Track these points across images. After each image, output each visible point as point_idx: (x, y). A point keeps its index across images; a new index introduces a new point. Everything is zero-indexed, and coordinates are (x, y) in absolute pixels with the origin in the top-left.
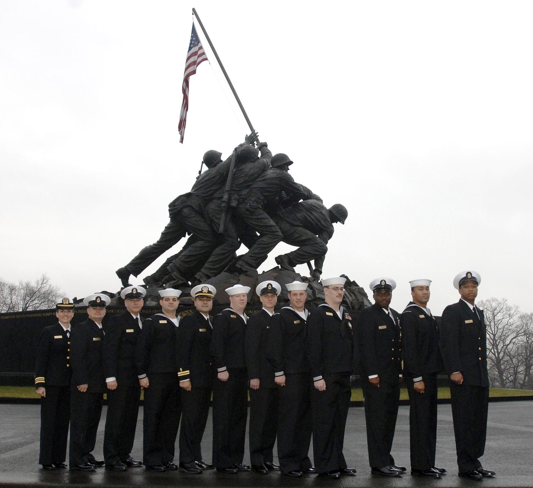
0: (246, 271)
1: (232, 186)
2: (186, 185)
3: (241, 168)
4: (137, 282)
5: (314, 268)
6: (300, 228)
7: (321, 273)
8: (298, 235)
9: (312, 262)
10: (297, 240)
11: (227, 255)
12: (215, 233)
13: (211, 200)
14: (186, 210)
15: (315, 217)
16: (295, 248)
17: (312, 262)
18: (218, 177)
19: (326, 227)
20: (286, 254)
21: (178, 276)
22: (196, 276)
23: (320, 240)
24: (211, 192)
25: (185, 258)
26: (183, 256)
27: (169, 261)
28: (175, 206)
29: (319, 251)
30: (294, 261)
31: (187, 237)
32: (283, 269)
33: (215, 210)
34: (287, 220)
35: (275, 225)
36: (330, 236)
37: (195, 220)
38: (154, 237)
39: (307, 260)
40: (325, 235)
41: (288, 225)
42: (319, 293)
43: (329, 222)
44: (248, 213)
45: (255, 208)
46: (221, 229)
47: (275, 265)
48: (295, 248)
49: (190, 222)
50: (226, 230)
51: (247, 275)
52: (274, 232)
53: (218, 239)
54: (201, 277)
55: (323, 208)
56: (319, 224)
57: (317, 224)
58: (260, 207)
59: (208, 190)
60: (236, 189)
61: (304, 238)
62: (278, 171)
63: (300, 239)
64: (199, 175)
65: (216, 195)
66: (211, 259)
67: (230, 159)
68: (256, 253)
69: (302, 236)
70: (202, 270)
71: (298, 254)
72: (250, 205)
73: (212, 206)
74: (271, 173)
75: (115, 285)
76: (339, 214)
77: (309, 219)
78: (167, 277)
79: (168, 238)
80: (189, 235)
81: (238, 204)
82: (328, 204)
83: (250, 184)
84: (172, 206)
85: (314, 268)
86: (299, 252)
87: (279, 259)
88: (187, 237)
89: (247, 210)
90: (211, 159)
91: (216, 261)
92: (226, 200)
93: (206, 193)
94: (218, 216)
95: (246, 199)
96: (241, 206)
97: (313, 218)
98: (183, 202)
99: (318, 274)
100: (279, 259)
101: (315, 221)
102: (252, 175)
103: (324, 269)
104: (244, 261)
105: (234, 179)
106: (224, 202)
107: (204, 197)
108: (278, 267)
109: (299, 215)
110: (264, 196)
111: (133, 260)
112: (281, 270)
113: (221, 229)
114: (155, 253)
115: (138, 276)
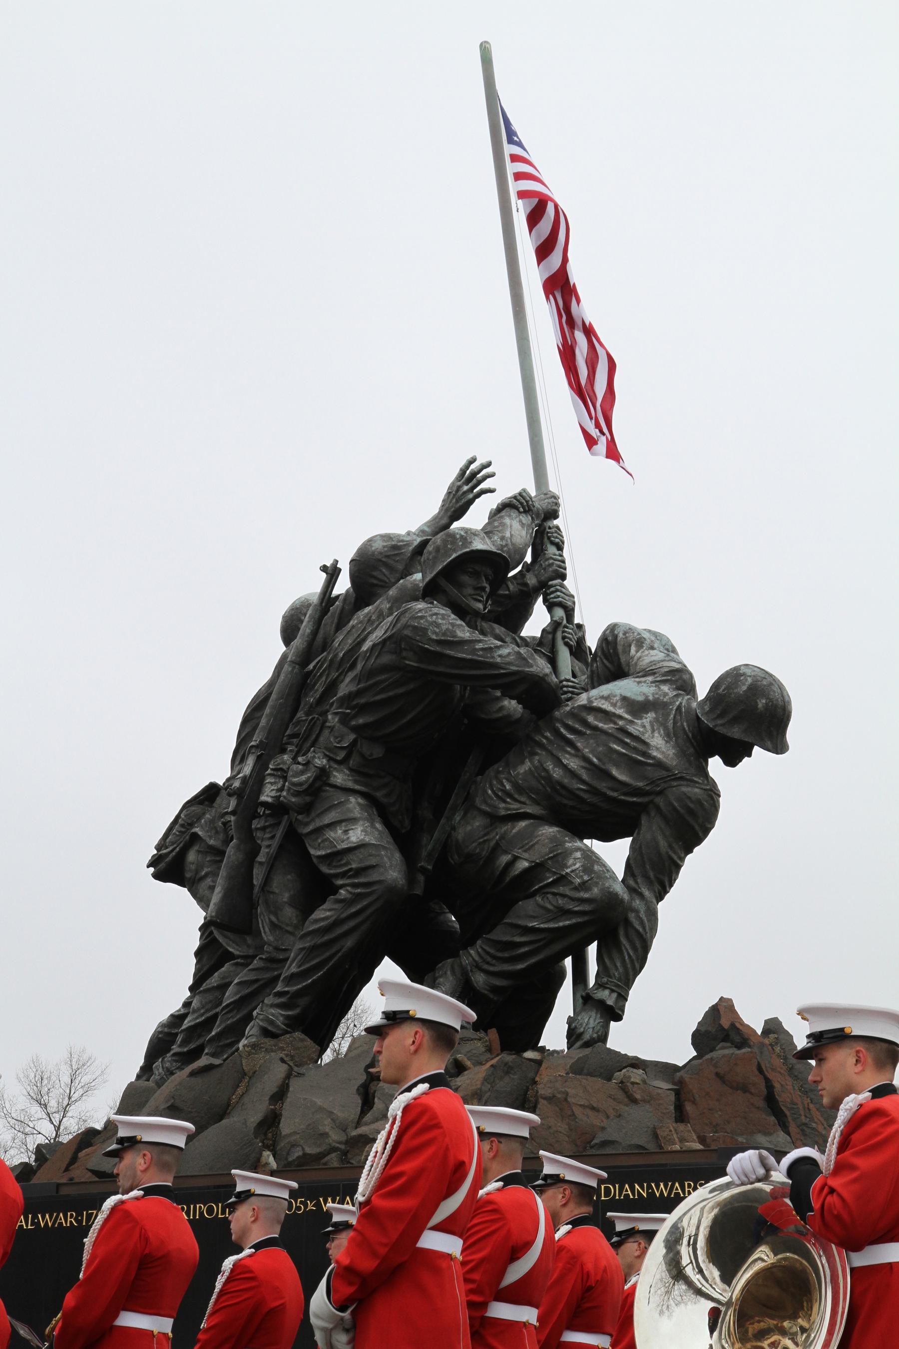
8: (505, 859)
29: (565, 913)
52: (359, 872)
56: (603, 786)
57: (594, 791)
69: (516, 859)
77: (557, 773)
97: (573, 763)
101: (585, 776)
110: (355, 729)
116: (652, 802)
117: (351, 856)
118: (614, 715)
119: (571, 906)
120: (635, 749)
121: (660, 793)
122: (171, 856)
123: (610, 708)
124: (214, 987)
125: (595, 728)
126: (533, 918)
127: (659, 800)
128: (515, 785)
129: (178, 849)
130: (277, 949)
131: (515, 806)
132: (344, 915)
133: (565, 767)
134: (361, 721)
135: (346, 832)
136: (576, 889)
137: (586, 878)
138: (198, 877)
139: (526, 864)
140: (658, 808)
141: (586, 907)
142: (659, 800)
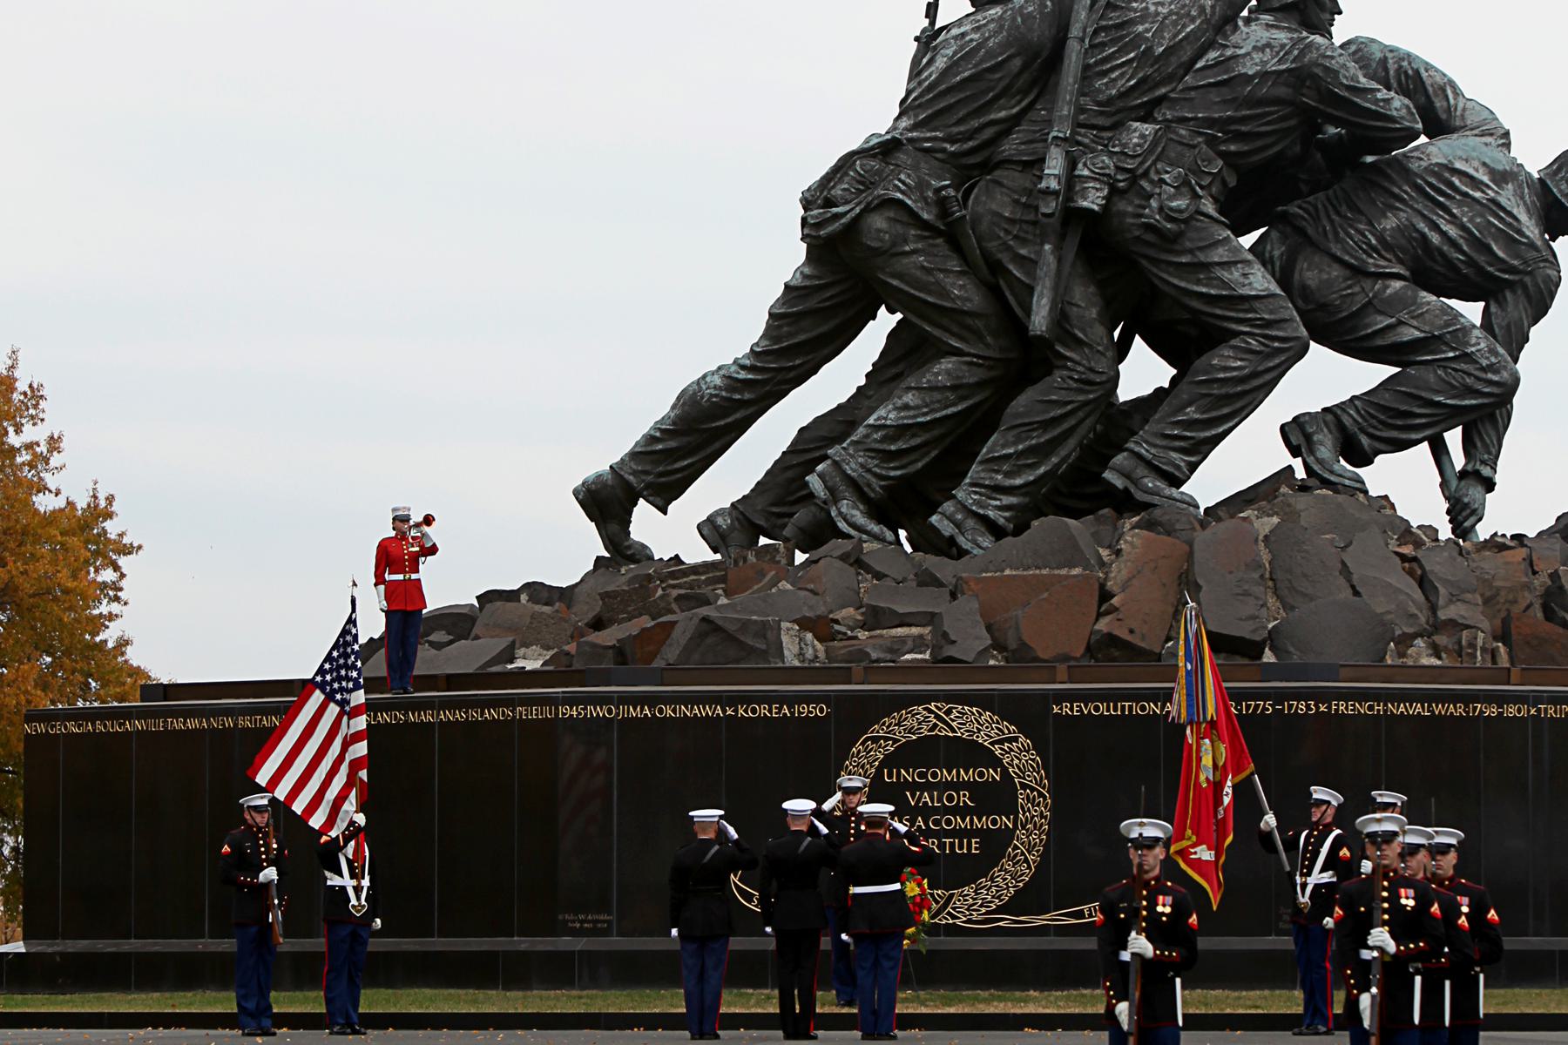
0: (1147, 506)
1: (1081, 110)
3: (1114, 18)
4: (671, 532)
5: (1458, 460)
6: (1398, 284)
7: (1490, 486)
9: (1454, 438)
10: (1379, 342)
11: (1066, 426)
12: (1014, 324)
13: (987, 167)
14: (878, 222)
15: (1463, 228)
16: (1369, 375)
17: (1454, 438)
18: (1017, 63)
19: (1512, 270)
20: (1325, 410)
21: (860, 519)
22: (934, 519)
23: (1479, 343)
24: (988, 133)
25: (883, 440)
26: (876, 428)
28: (829, 203)
30: (1365, 440)
31: (885, 322)
32: (1313, 482)
33: (1011, 221)
34: (1336, 250)
35: (1275, 288)
36: (1540, 305)
37: (919, 258)
38: (734, 333)
39: (1428, 432)
40: (1515, 306)
41: (1336, 272)
42: (1453, 599)
43: (1531, 245)
44: (1149, 237)
45: (1185, 221)
46: (1039, 320)
47: (1279, 457)
48: (1369, 375)
49: (894, 276)
50: (1061, 318)
51: (1150, 525)
52: (1269, 324)
54: (958, 525)
55: (1508, 175)
56: (1481, 259)
57: (1471, 262)
58: (1209, 207)
59: (975, 123)
60: (1101, 121)
61: (1410, 334)
62: (1282, 36)
63: (1391, 338)
64: (926, 22)
65: (1011, 147)
66: (995, 445)
68: (1191, 424)
69: (1400, 323)
70: (960, 494)
71: (1384, 409)
72: (1161, 209)
73: (993, 202)
75: (570, 552)
77: (1435, 238)
78: (802, 515)
80: (892, 311)
81: (1108, 198)
83: (1163, 90)
84: (817, 199)
85: (1458, 460)
86: (1386, 399)
87: (1297, 434)
88: (885, 322)
89: (1149, 227)
91: (1019, 455)
92: (1054, 185)
93: (970, 139)
94: (1023, 252)
95: (1146, 174)
96: (1122, 205)
97: (1452, 231)
98: (866, 184)
99: (1473, 492)
100: (1297, 434)
102: (1169, 51)
103: (1506, 470)
104: (1139, 456)
105: (1088, 74)
106: (1047, 192)
107: (953, 154)
108: (1290, 467)
109: (1389, 223)
110: (1223, 155)
111: (650, 439)
112: (1303, 488)
113: (1039, 320)
114: (743, 404)
115: (673, 507)
116: (1521, 281)
117: (1257, 305)
118: (1482, 182)
119: (1479, 386)
120: (1509, 225)
121: (1530, 273)
122: (852, 214)
123: (1471, 171)
124: (945, 387)
125: (1466, 195)
126: (1438, 392)
127: (1527, 279)
128: (1381, 238)
129: (858, 210)
130: (1091, 370)
131: (1383, 263)
132: (1261, 368)
133: (1443, 234)
134: (1232, 148)
135: (1245, 275)
136: (1483, 369)
137: (1493, 360)
138: (894, 250)
139: (1417, 334)
140: (1525, 287)
141: (1495, 390)
142: (1527, 279)
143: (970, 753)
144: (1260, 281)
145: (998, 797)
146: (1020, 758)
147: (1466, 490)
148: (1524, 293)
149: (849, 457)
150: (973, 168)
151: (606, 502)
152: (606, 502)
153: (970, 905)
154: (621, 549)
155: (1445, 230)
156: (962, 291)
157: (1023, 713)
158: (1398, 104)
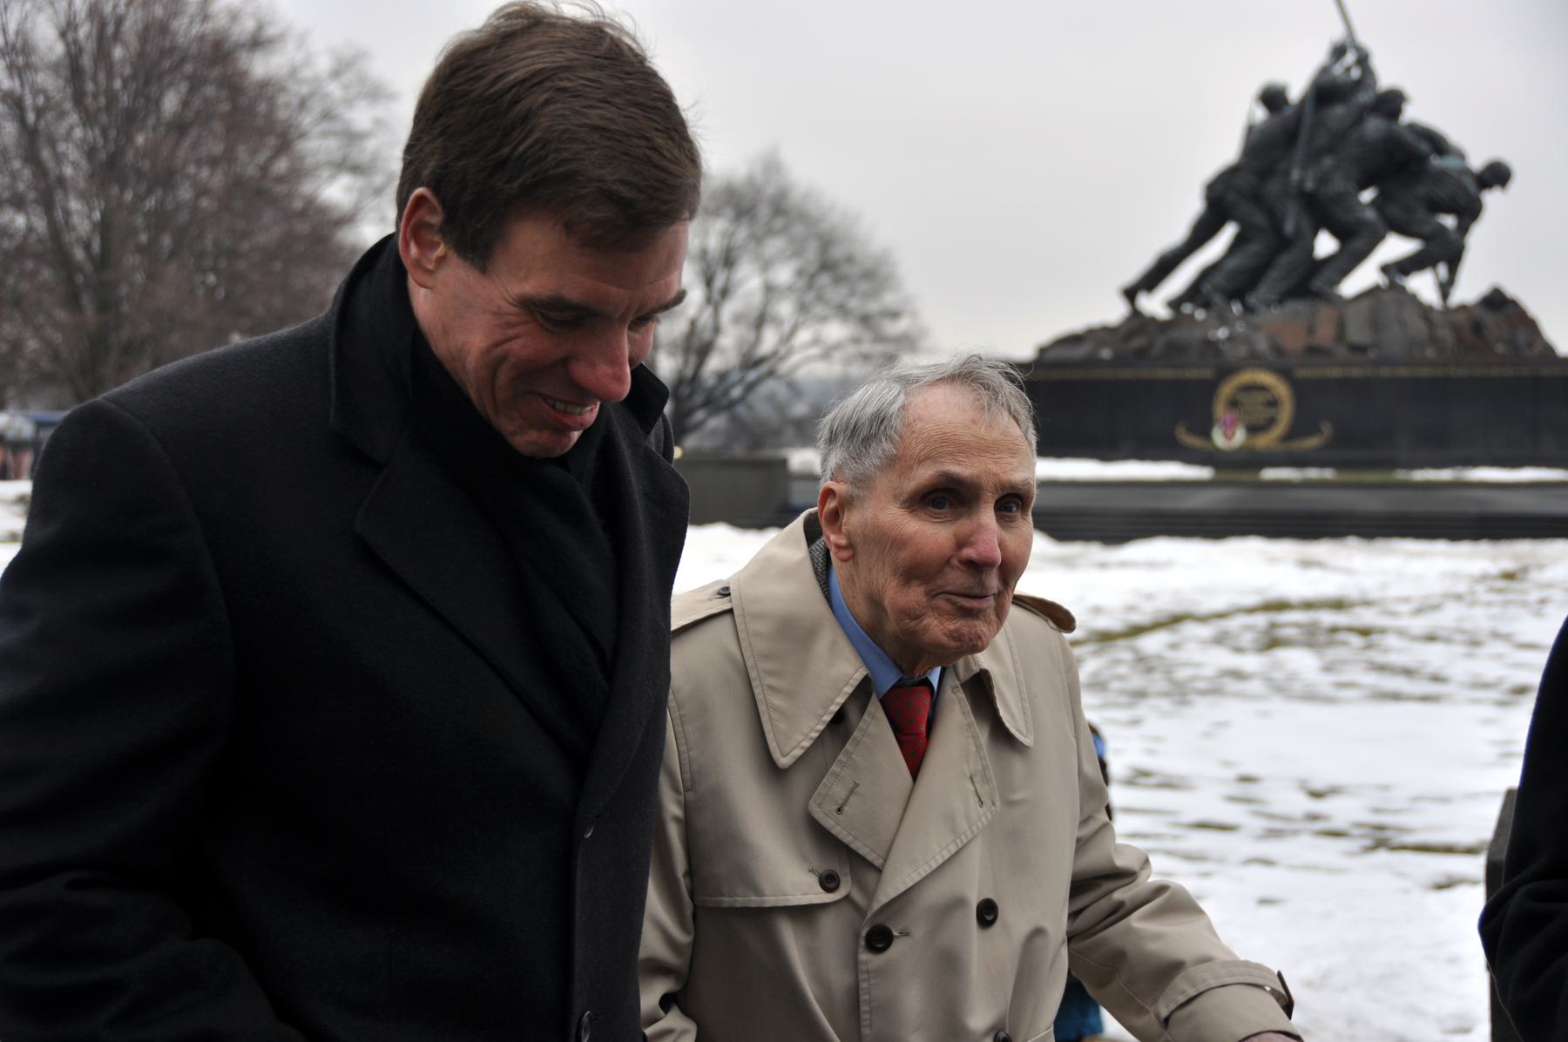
2: (1226, 150)
4: (1155, 305)
9: (1442, 270)
12: (1277, 227)
27: (1207, 273)
38: (1178, 233)
53: (1282, 243)
55: (1467, 171)
67: (1303, 102)
73: (1273, 187)
74: (1374, 126)
75: (1114, 312)
76: (1497, 175)
79: (1202, 233)
82: (1477, 161)
87: (1385, 269)
90: (1272, 98)
100: (1385, 269)
113: (1289, 227)
143: (1261, 388)
144: (1370, 215)
145: (1274, 403)
146: (1281, 389)
147: (1445, 288)
148: (1470, 212)
149: (1218, 279)
150: (1265, 174)
151: (1130, 294)
152: (1130, 294)
153: (1265, 441)
154: (1136, 314)
155: (1442, 193)
156: (1260, 219)
157: (1285, 373)
158: (1424, 147)
